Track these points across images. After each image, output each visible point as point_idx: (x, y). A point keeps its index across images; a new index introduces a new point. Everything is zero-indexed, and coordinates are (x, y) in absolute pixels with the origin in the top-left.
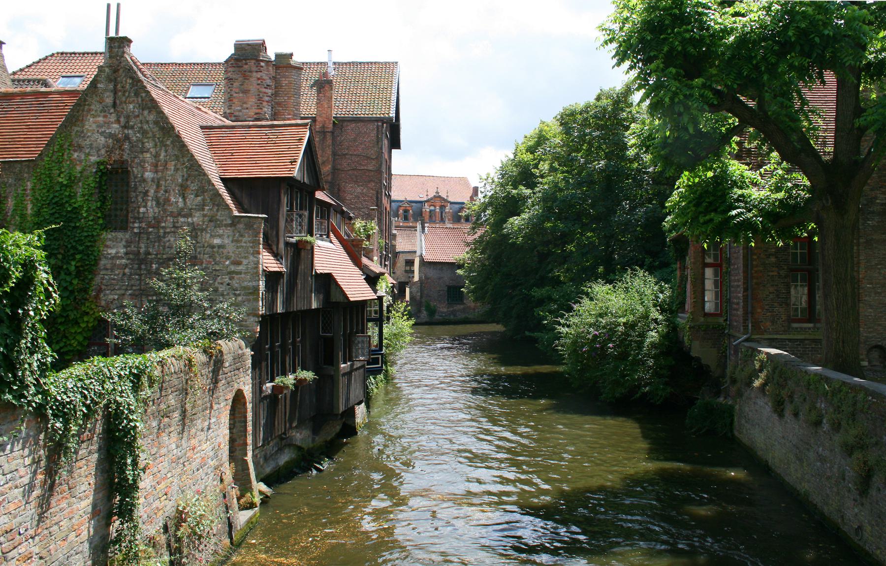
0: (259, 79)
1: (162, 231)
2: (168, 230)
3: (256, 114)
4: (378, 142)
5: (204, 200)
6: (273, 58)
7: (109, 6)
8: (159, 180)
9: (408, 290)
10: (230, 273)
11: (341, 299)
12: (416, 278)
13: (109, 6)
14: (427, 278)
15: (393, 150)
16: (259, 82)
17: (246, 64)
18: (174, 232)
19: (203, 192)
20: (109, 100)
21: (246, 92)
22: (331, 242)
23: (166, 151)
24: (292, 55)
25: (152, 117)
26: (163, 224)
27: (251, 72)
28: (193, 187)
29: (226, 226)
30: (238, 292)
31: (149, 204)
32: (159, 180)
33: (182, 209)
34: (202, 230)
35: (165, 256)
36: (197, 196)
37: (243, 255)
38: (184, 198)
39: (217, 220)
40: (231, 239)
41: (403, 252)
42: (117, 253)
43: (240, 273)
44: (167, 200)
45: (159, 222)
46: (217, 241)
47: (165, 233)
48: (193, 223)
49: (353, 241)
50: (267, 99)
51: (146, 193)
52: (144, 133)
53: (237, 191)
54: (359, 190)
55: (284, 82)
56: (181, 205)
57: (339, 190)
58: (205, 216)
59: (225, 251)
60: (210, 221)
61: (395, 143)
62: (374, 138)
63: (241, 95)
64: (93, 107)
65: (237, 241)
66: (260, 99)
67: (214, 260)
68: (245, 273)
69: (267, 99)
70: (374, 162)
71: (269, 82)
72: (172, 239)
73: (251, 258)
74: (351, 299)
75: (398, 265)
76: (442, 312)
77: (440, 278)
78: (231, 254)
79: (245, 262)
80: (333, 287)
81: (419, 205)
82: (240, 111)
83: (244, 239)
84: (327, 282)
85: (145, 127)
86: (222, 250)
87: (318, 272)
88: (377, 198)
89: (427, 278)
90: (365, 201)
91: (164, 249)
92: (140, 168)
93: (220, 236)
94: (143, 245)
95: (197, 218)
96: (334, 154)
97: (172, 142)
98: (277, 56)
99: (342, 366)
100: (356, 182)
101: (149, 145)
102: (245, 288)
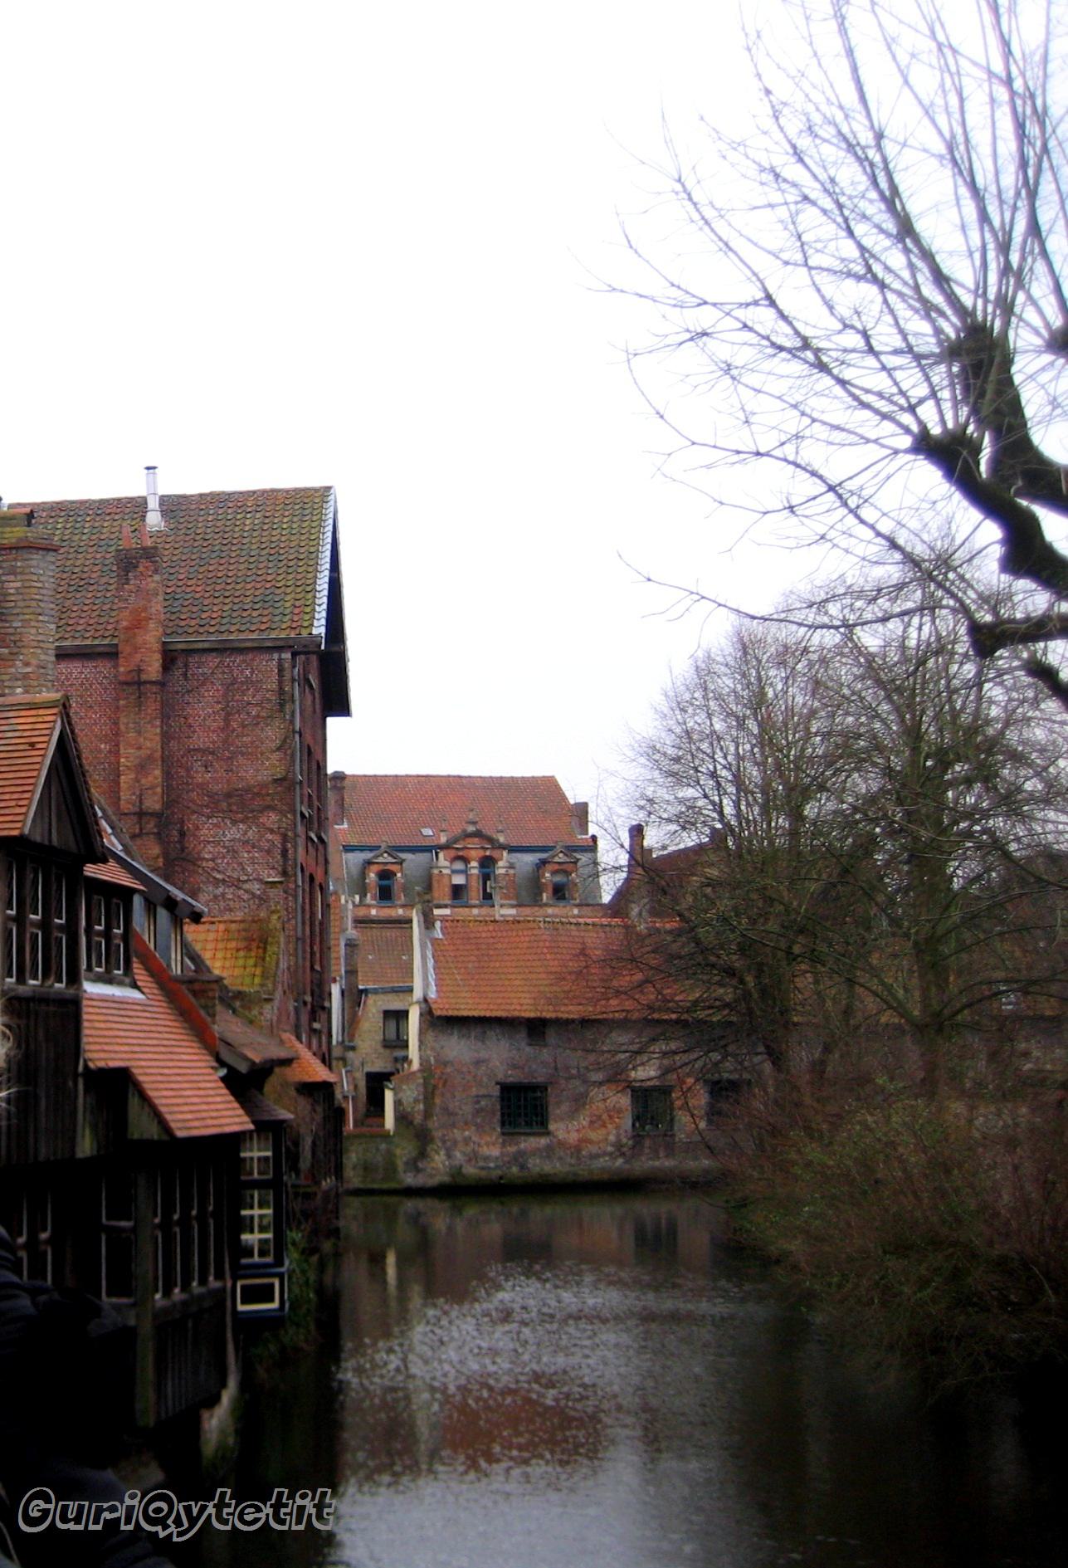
4: (282, 705)
9: (389, 1096)
11: (153, 1132)
12: (416, 1066)
15: (329, 720)
22: (135, 986)
41: (375, 992)
57: (182, 834)
61: (336, 700)
74: (180, 1134)
76: (487, 1159)
77: (478, 1063)
80: (134, 1102)
84: (117, 1085)
87: (91, 1065)
88: (284, 852)
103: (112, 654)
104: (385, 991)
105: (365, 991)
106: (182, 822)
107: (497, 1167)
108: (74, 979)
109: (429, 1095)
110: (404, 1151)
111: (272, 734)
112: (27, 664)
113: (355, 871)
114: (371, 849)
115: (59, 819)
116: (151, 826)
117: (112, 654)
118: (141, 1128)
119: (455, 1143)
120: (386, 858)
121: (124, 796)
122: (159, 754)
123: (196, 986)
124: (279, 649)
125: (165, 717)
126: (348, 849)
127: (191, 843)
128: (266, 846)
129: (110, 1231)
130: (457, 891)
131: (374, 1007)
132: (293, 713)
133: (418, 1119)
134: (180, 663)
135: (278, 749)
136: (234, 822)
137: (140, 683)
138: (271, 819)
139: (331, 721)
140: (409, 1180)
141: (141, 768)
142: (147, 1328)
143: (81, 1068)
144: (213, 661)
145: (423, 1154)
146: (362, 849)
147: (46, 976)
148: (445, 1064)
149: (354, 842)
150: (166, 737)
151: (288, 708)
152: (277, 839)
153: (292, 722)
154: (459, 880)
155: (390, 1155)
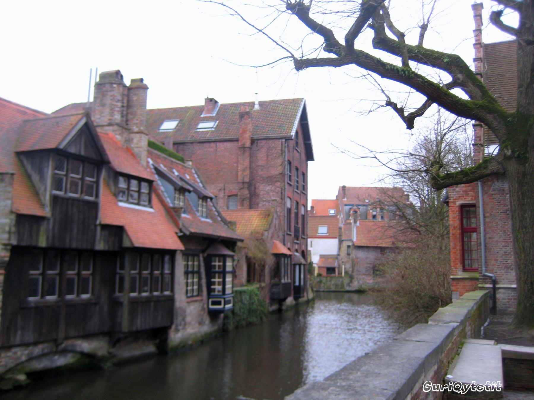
0: (111, 96)
4: (282, 154)
7: (91, 69)
13: (91, 69)
16: (112, 98)
17: (105, 87)
21: (103, 105)
24: (142, 80)
27: (107, 91)
49: (174, 208)
50: (117, 109)
53: (25, 162)
55: (135, 98)
57: (255, 188)
61: (310, 156)
66: (112, 110)
69: (117, 109)
71: (119, 98)
75: (342, 249)
77: (367, 258)
81: (365, 207)
82: (99, 119)
88: (282, 193)
98: (133, 81)
99: (133, 295)
103: (237, 140)
104: (348, 240)
105: (343, 240)
106: (255, 185)
108: (97, 196)
109: (353, 267)
110: (346, 281)
111: (279, 161)
113: (347, 211)
114: (352, 205)
115: (86, 147)
116: (246, 186)
117: (237, 140)
118: (126, 244)
119: (360, 279)
120: (355, 207)
121: (239, 178)
122: (248, 167)
124: (282, 138)
125: (251, 157)
126: (346, 205)
127: (257, 191)
128: (277, 191)
129: (119, 274)
130: (374, 217)
131: (345, 244)
132: (285, 155)
133: (350, 273)
134: (256, 142)
135: (281, 165)
136: (269, 185)
137: (244, 148)
138: (278, 184)
139: (310, 163)
140: (348, 288)
141: (244, 170)
142: (126, 302)
143: (98, 222)
144: (264, 142)
145: (351, 282)
146: (349, 205)
147: (82, 193)
148: (358, 258)
149: (347, 203)
150: (251, 162)
151: (284, 154)
152: (280, 189)
153: (284, 158)
154: (374, 213)
155: (342, 281)
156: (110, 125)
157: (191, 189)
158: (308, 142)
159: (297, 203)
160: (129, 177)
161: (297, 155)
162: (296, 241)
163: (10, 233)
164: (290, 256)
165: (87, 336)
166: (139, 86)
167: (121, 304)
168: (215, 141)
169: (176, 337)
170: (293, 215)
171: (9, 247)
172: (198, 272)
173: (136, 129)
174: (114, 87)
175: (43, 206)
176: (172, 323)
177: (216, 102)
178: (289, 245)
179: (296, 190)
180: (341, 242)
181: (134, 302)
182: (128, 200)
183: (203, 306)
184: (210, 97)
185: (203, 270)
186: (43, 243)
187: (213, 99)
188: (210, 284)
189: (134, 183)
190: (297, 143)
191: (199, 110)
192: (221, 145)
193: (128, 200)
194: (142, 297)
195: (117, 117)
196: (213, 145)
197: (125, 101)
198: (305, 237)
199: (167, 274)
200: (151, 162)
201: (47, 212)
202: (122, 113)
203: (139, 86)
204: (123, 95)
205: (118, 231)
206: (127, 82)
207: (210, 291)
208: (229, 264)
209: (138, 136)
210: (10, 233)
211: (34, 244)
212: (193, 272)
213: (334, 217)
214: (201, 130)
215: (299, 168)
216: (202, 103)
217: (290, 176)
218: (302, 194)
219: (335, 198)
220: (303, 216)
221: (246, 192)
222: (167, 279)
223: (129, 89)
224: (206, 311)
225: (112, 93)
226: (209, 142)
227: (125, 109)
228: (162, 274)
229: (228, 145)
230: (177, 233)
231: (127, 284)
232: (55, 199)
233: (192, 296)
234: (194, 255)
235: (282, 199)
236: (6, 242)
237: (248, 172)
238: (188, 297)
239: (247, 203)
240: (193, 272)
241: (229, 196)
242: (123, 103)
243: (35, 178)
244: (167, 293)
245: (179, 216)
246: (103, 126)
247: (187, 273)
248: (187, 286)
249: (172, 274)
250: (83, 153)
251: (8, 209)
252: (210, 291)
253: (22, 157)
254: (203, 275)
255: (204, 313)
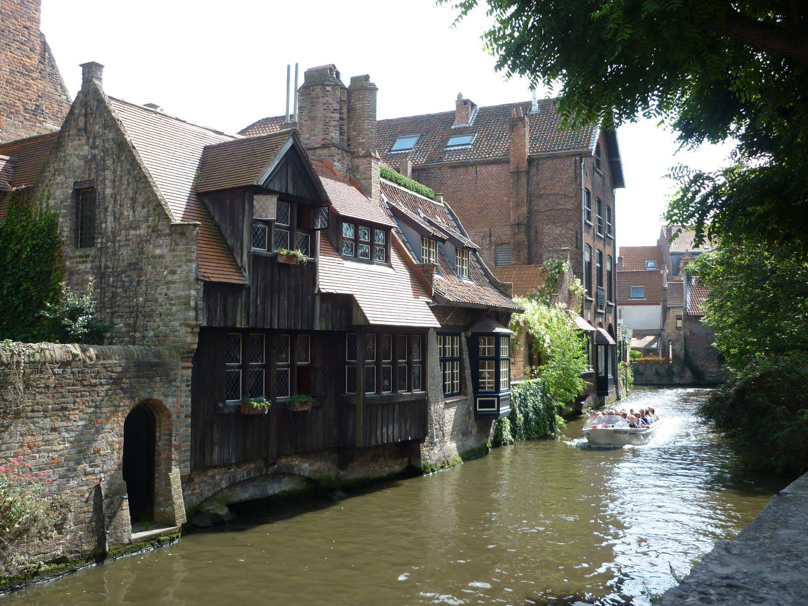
0: (324, 104)
1: (117, 245)
2: (122, 244)
3: (323, 140)
4: (576, 178)
5: (148, 211)
6: (347, 83)
7: (289, 67)
8: (115, 195)
10: (167, 283)
13: (289, 67)
14: (692, 334)
18: (126, 245)
19: (148, 204)
20: (81, 124)
21: (313, 119)
22: (393, 268)
23: (121, 166)
24: (367, 77)
25: (111, 135)
26: (118, 238)
27: (317, 97)
28: (141, 199)
29: (166, 235)
30: (173, 302)
31: (109, 219)
32: (115, 195)
33: (132, 222)
34: (148, 241)
35: (119, 269)
36: (143, 208)
37: (178, 264)
38: (134, 212)
39: (158, 231)
40: (168, 248)
42: (86, 268)
43: (173, 282)
44: (121, 214)
45: (115, 237)
46: (158, 252)
47: (120, 246)
48: (140, 235)
50: (334, 123)
51: (106, 209)
52: (105, 151)
54: (557, 231)
55: (359, 105)
56: (131, 218)
58: (149, 227)
59: (164, 261)
60: (153, 231)
61: (617, 179)
62: (572, 175)
63: (309, 122)
64: (71, 132)
65: (173, 250)
67: (156, 270)
68: (179, 282)
69: (334, 123)
70: (572, 201)
71: (337, 106)
72: (125, 252)
73: (184, 267)
74: (371, 322)
75: (668, 321)
76: (712, 373)
78: (168, 264)
79: (179, 270)
80: (355, 309)
82: (309, 139)
83: (179, 248)
85: (107, 146)
86: (161, 260)
88: (577, 239)
89: (692, 334)
90: (564, 242)
91: (118, 262)
92: (102, 186)
93: (160, 246)
94: (103, 260)
95: (142, 231)
96: (529, 195)
97: (126, 157)
98: (354, 80)
100: (554, 223)
101: (109, 162)
102: (179, 298)
105: (669, 308)
107: (716, 377)
108: (313, 254)
112: (363, 138)
116: (523, 228)
118: (357, 321)
123: (425, 268)
124: (574, 156)
129: (348, 364)
131: (672, 314)
134: (535, 163)
136: (557, 227)
139: (618, 192)
143: (316, 291)
144: (549, 162)
151: (578, 180)
156: (324, 146)
157: (446, 237)
158: (615, 160)
159: (601, 254)
160: (356, 223)
161: (599, 179)
162: (599, 311)
163: (196, 309)
164: (592, 332)
165: (305, 453)
166: (363, 88)
167: (354, 407)
168: (474, 164)
169: (431, 454)
170: (594, 272)
171: (197, 330)
172: (460, 359)
173: (362, 152)
174: (328, 91)
175: (239, 270)
176: (426, 434)
177: (473, 105)
178: (589, 315)
179: (598, 234)
180: (665, 310)
181: (370, 405)
182: (356, 256)
183: (468, 408)
184: (465, 98)
185: (466, 357)
186: (241, 323)
187: (468, 100)
188: (476, 376)
189: (362, 230)
190: (598, 162)
191: (446, 119)
192: (483, 170)
193: (356, 256)
194: (382, 397)
195: (335, 135)
196: (471, 170)
197: (345, 111)
198: (614, 304)
199: (417, 363)
200: (386, 200)
201: (244, 279)
202: (341, 129)
203: (363, 88)
204: (341, 101)
205: (345, 304)
206: (347, 83)
207: (477, 386)
208: (504, 347)
209: (365, 160)
210: (196, 309)
211: (230, 324)
212: (452, 359)
213: (656, 273)
214: (452, 149)
215: (602, 198)
216: (451, 107)
217: (589, 213)
218: (607, 239)
219: (655, 244)
220: (610, 273)
221: (522, 237)
222: (416, 368)
223: (349, 91)
224: (473, 415)
225: (325, 100)
226: (464, 165)
227: (345, 122)
228: (409, 363)
229: (494, 169)
230: (428, 303)
231: (361, 379)
232: (256, 259)
233: (453, 395)
234: (452, 335)
235: (577, 247)
236: (193, 323)
237: (524, 209)
238: (446, 396)
239: (524, 254)
240: (452, 359)
241: (497, 245)
242: (341, 113)
243: (227, 230)
244: (417, 392)
245: (431, 278)
246: (315, 149)
247: (443, 360)
248: (444, 380)
249: (424, 363)
250: (290, 191)
251: (192, 276)
252: (477, 386)
253: (207, 201)
254: (467, 364)
255: (469, 419)
